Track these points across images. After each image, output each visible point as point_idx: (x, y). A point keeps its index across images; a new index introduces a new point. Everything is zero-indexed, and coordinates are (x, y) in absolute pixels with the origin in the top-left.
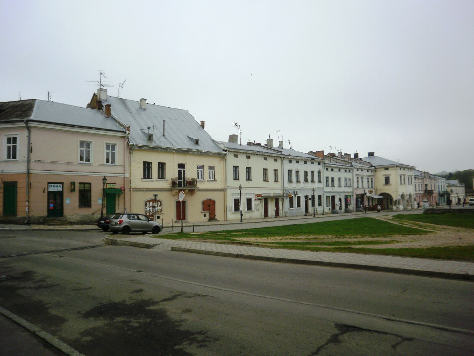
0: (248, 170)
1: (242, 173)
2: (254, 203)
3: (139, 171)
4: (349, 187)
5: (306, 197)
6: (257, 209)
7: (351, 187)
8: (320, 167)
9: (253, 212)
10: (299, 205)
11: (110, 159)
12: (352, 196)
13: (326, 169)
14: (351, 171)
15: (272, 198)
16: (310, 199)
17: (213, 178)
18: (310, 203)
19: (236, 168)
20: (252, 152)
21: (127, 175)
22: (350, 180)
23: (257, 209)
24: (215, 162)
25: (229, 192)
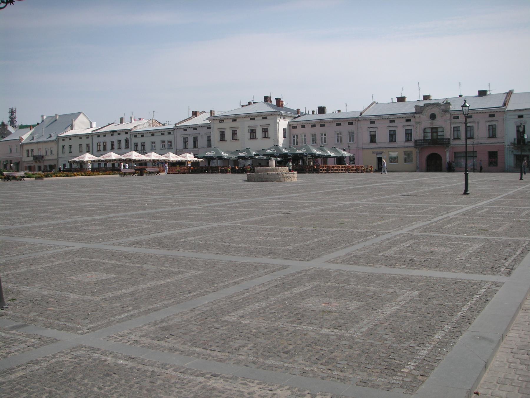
3: (25, 154)
7: (172, 148)
8: (128, 136)
13: (134, 137)
14: (172, 133)
22: (169, 142)
25: (60, 160)
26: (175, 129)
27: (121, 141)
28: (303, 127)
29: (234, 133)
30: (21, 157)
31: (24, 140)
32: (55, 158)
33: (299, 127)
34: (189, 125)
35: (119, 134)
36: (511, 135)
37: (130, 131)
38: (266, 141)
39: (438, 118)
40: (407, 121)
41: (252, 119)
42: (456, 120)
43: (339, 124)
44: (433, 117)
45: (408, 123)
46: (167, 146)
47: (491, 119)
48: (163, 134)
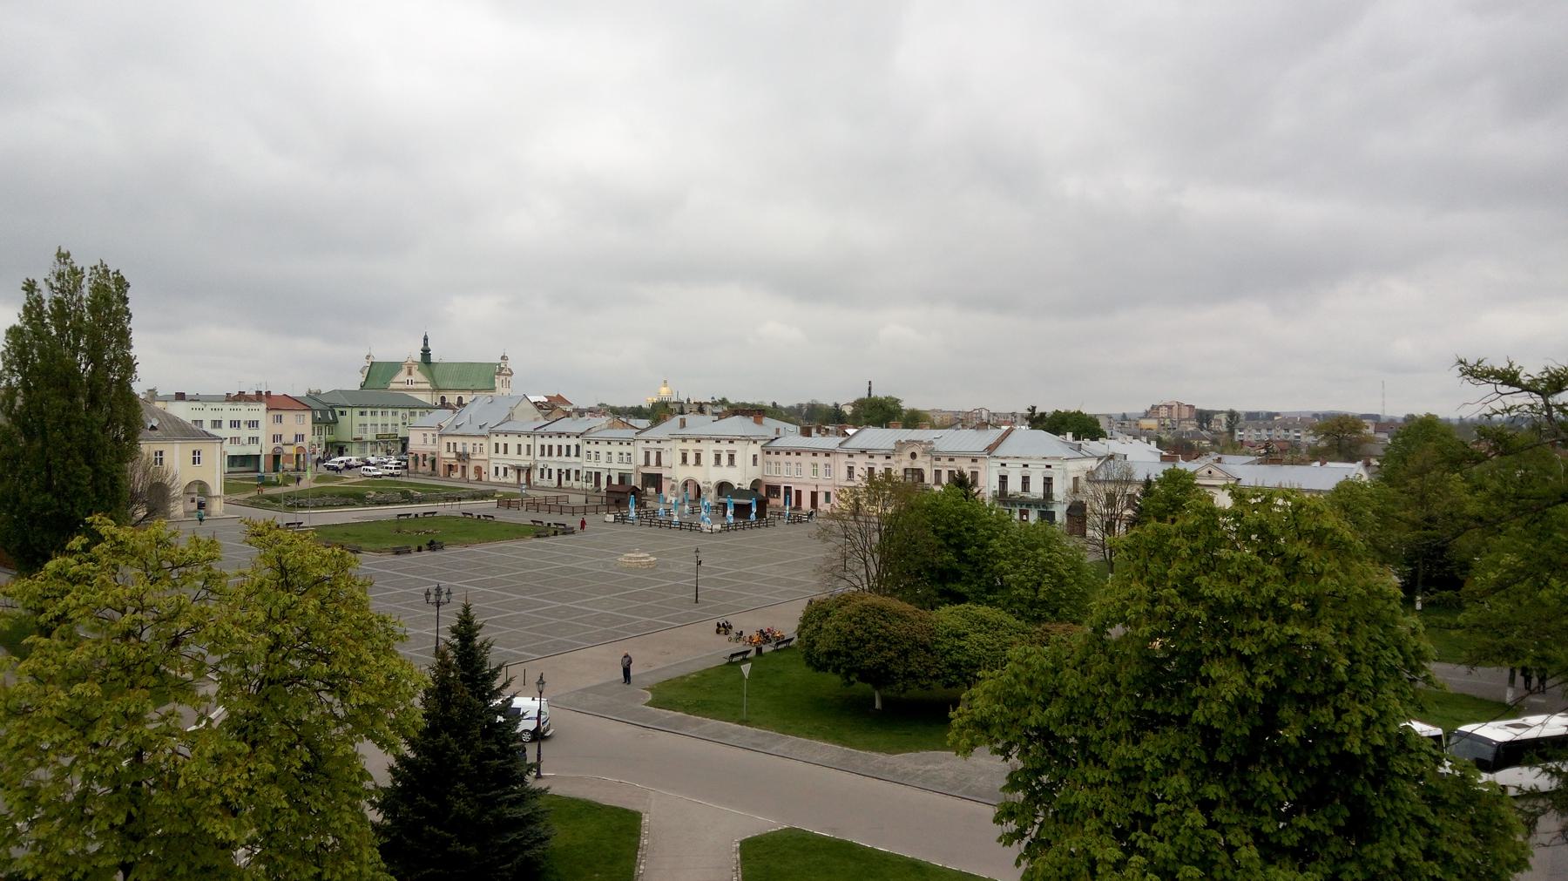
3: (445, 448)
5: (559, 470)
8: (579, 441)
10: (550, 477)
11: (434, 441)
18: (564, 477)
19: (497, 445)
24: (482, 440)
25: (492, 462)
28: (777, 453)
29: (698, 456)
33: (773, 453)
35: (568, 437)
36: (995, 485)
38: (731, 470)
39: (919, 457)
40: (888, 457)
41: (718, 441)
42: (939, 463)
43: (815, 454)
44: (913, 455)
45: (888, 461)
46: (625, 460)
47: (974, 464)
48: (621, 444)
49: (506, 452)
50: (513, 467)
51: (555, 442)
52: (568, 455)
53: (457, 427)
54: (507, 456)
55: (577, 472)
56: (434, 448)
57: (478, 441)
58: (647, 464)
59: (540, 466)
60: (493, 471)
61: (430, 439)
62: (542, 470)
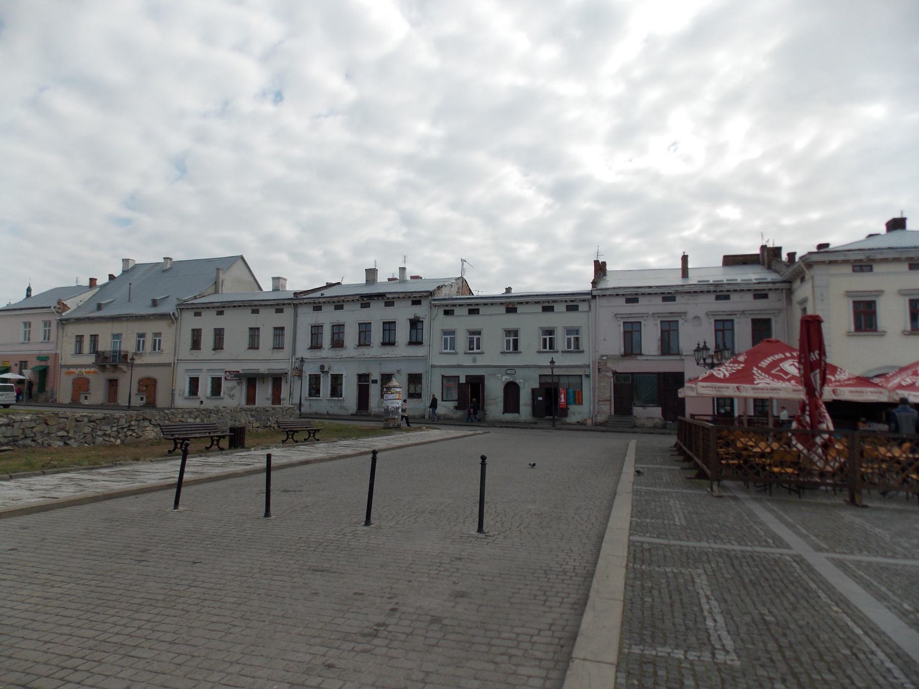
0: (219, 334)
1: (207, 340)
2: (224, 384)
3: (69, 346)
4: (562, 352)
6: (231, 394)
8: (420, 311)
9: (222, 398)
11: (47, 337)
12: (583, 377)
14: (583, 307)
15: (263, 377)
16: (375, 382)
17: (159, 349)
20: (218, 304)
21: (58, 352)
22: (569, 331)
23: (231, 394)
24: (161, 326)
25: (181, 368)
26: (594, 297)
27: (395, 322)
30: (56, 354)
31: (68, 312)
32: (167, 362)
34: (650, 287)
37: (432, 296)
49: (218, 345)
50: (238, 376)
51: (351, 317)
52: (388, 343)
53: (99, 307)
54: (221, 355)
55: (415, 379)
56: (47, 349)
57: (149, 328)
58: (631, 348)
59: (310, 369)
60: (184, 385)
61: (38, 331)
62: (315, 381)
